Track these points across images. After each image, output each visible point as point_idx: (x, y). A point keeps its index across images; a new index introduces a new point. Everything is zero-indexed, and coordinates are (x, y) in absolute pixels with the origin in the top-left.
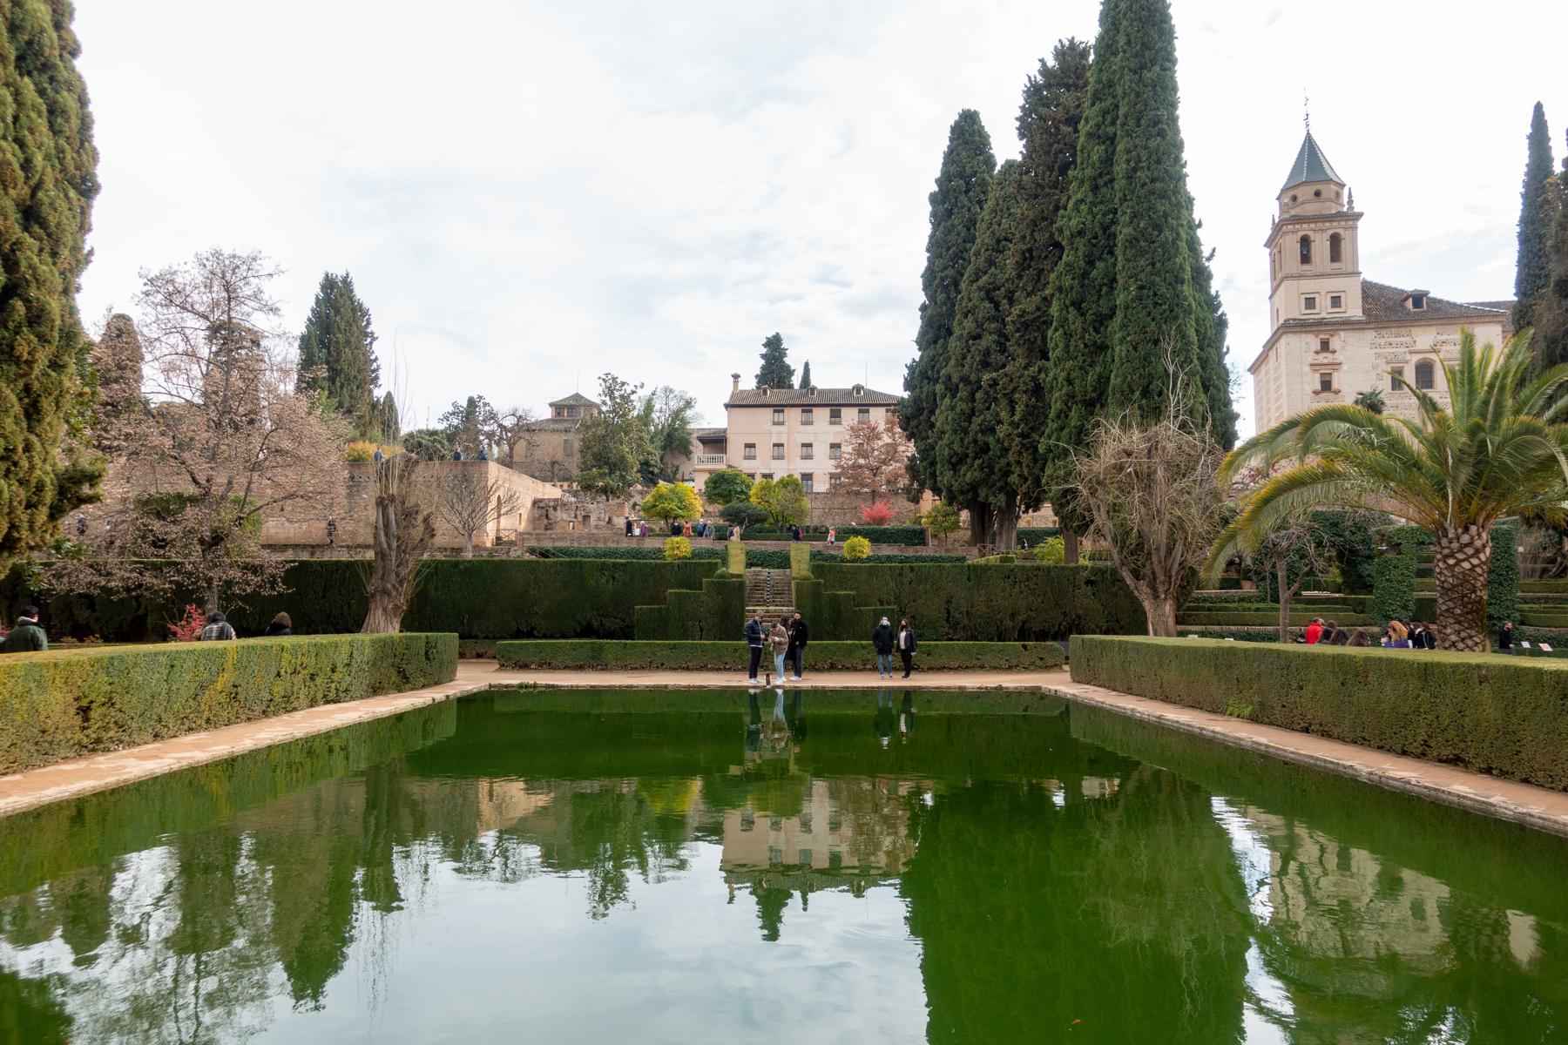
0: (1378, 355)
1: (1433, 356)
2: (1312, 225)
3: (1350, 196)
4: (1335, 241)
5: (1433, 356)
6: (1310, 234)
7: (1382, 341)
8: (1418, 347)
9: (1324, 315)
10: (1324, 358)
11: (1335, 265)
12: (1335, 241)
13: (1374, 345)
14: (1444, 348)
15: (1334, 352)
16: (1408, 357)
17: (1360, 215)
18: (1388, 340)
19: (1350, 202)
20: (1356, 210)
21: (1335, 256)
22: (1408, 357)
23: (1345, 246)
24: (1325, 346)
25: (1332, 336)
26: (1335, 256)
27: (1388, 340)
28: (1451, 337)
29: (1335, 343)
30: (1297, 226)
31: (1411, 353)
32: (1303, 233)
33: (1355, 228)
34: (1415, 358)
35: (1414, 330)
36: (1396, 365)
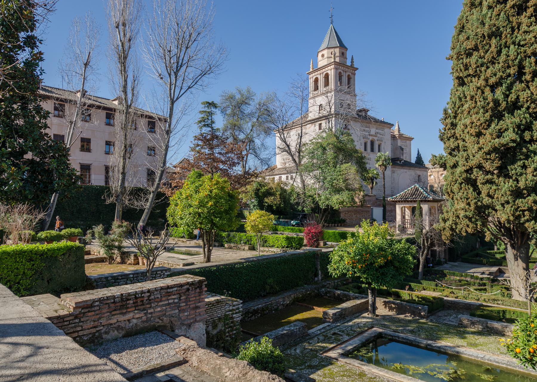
1: (374, 138)
2: (343, 68)
4: (349, 78)
6: (342, 72)
7: (362, 128)
8: (371, 133)
12: (349, 78)
15: (349, 129)
16: (369, 137)
17: (357, 69)
18: (364, 128)
19: (352, 62)
20: (355, 66)
22: (369, 137)
24: (346, 127)
27: (364, 128)
31: (369, 135)
32: (339, 71)
33: (354, 74)
34: (371, 138)
36: (366, 140)
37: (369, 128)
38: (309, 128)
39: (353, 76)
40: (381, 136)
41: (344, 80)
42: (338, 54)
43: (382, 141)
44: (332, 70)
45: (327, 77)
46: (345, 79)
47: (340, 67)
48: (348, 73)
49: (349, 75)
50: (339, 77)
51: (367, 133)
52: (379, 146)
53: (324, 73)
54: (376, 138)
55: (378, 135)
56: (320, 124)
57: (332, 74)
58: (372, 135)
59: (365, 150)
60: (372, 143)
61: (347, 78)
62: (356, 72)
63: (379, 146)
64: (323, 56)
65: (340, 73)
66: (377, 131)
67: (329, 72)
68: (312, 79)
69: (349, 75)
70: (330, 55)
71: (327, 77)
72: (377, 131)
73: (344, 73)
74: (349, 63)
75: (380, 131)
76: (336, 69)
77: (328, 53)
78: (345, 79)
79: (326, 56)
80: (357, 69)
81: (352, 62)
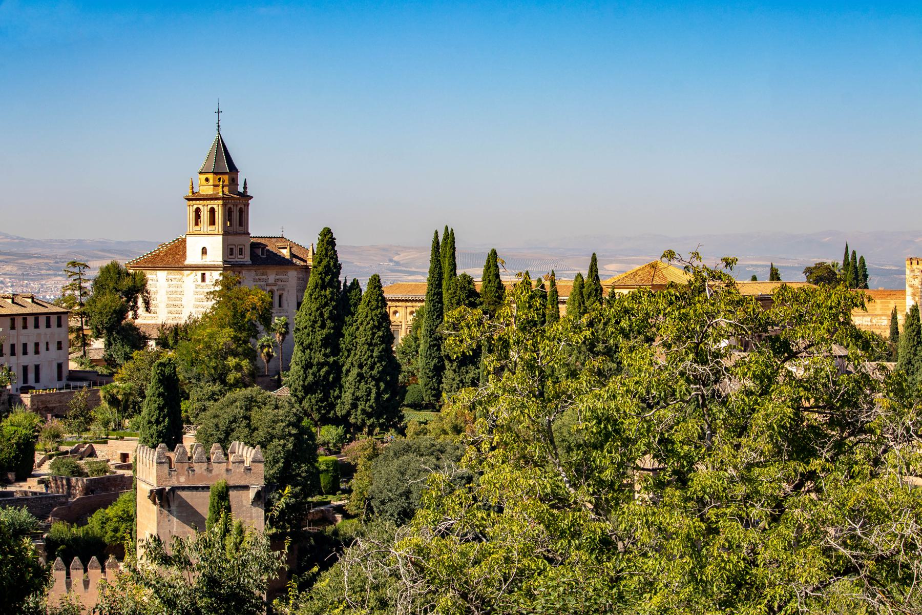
3: (245, 184)
4: (241, 211)
7: (257, 277)
8: (270, 282)
9: (237, 260)
11: (241, 228)
13: (255, 280)
14: (278, 283)
17: (252, 197)
19: (245, 188)
21: (241, 224)
31: (267, 285)
32: (229, 206)
33: (248, 204)
38: (188, 275)
40: (283, 283)
42: (227, 183)
43: (283, 290)
44: (220, 207)
45: (212, 211)
46: (236, 215)
49: (241, 209)
50: (228, 215)
51: (264, 283)
52: (280, 297)
53: (209, 207)
54: (275, 288)
56: (203, 275)
57: (220, 212)
62: (250, 201)
63: (280, 297)
64: (207, 180)
65: (230, 208)
67: (215, 207)
69: (241, 209)
70: (217, 183)
71: (212, 211)
74: (241, 189)
76: (224, 205)
77: (214, 179)
78: (236, 215)
79: (211, 182)
80: (252, 197)
81: (245, 188)
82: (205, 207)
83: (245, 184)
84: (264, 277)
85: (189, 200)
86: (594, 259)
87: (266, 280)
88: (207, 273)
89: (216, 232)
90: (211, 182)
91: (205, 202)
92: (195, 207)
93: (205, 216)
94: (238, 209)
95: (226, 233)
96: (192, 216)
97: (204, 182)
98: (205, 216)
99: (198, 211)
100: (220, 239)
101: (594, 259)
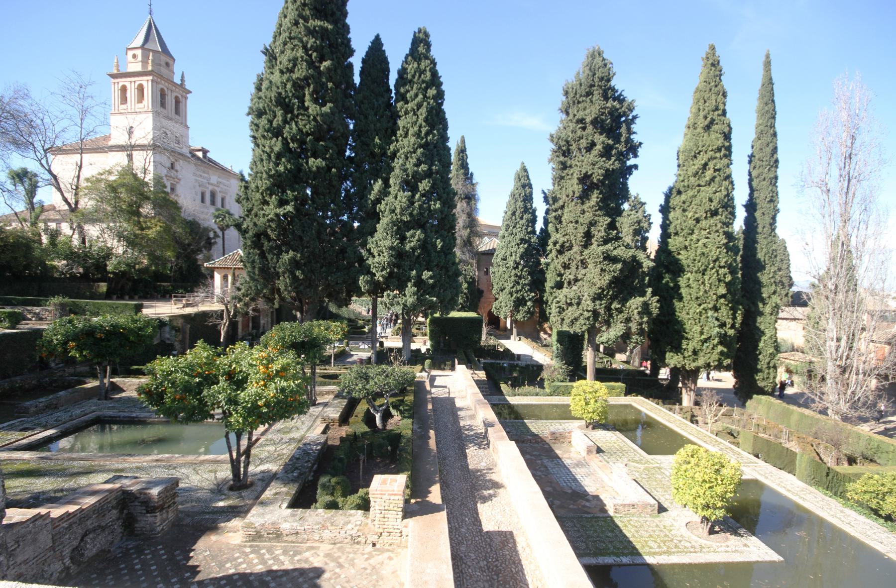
0: (196, 181)
2: (167, 84)
3: (183, 76)
4: (177, 102)
5: (216, 188)
6: (166, 89)
7: (198, 173)
10: (173, 173)
11: (177, 117)
12: (177, 102)
13: (195, 174)
14: (221, 186)
15: (177, 171)
16: (207, 185)
17: (190, 92)
19: (182, 80)
21: (177, 112)
22: (207, 185)
23: (181, 105)
24: (172, 166)
25: (176, 160)
26: (177, 112)
28: (223, 181)
29: (177, 167)
30: (159, 80)
31: (209, 183)
32: (161, 86)
33: (186, 98)
34: (211, 188)
35: (210, 171)
37: (208, 174)
39: (184, 99)
41: (170, 103)
43: (226, 193)
44: (150, 83)
45: (141, 89)
47: (163, 82)
48: (174, 94)
49: (177, 98)
51: (205, 181)
54: (218, 189)
55: (221, 186)
58: (212, 184)
59: (203, 201)
60: (213, 195)
61: (174, 101)
62: (188, 95)
64: (134, 56)
66: (220, 180)
67: (145, 84)
68: (116, 85)
69: (177, 98)
71: (141, 89)
72: (220, 180)
73: (170, 92)
75: (223, 181)
80: (190, 92)
81: (182, 80)
82: (133, 84)
83: (183, 76)
84: (206, 175)
85: (113, 76)
86: (768, 56)
87: (209, 179)
88: (135, 153)
89: (146, 109)
90: (140, 58)
91: (133, 79)
92: (121, 84)
93: (131, 94)
94: (173, 97)
95: (156, 114)
96: (117, 94)
97: (133, 60)
98: (131, 94)
99: (124, 89)
100: (151, 115)
101: (768, 56)
